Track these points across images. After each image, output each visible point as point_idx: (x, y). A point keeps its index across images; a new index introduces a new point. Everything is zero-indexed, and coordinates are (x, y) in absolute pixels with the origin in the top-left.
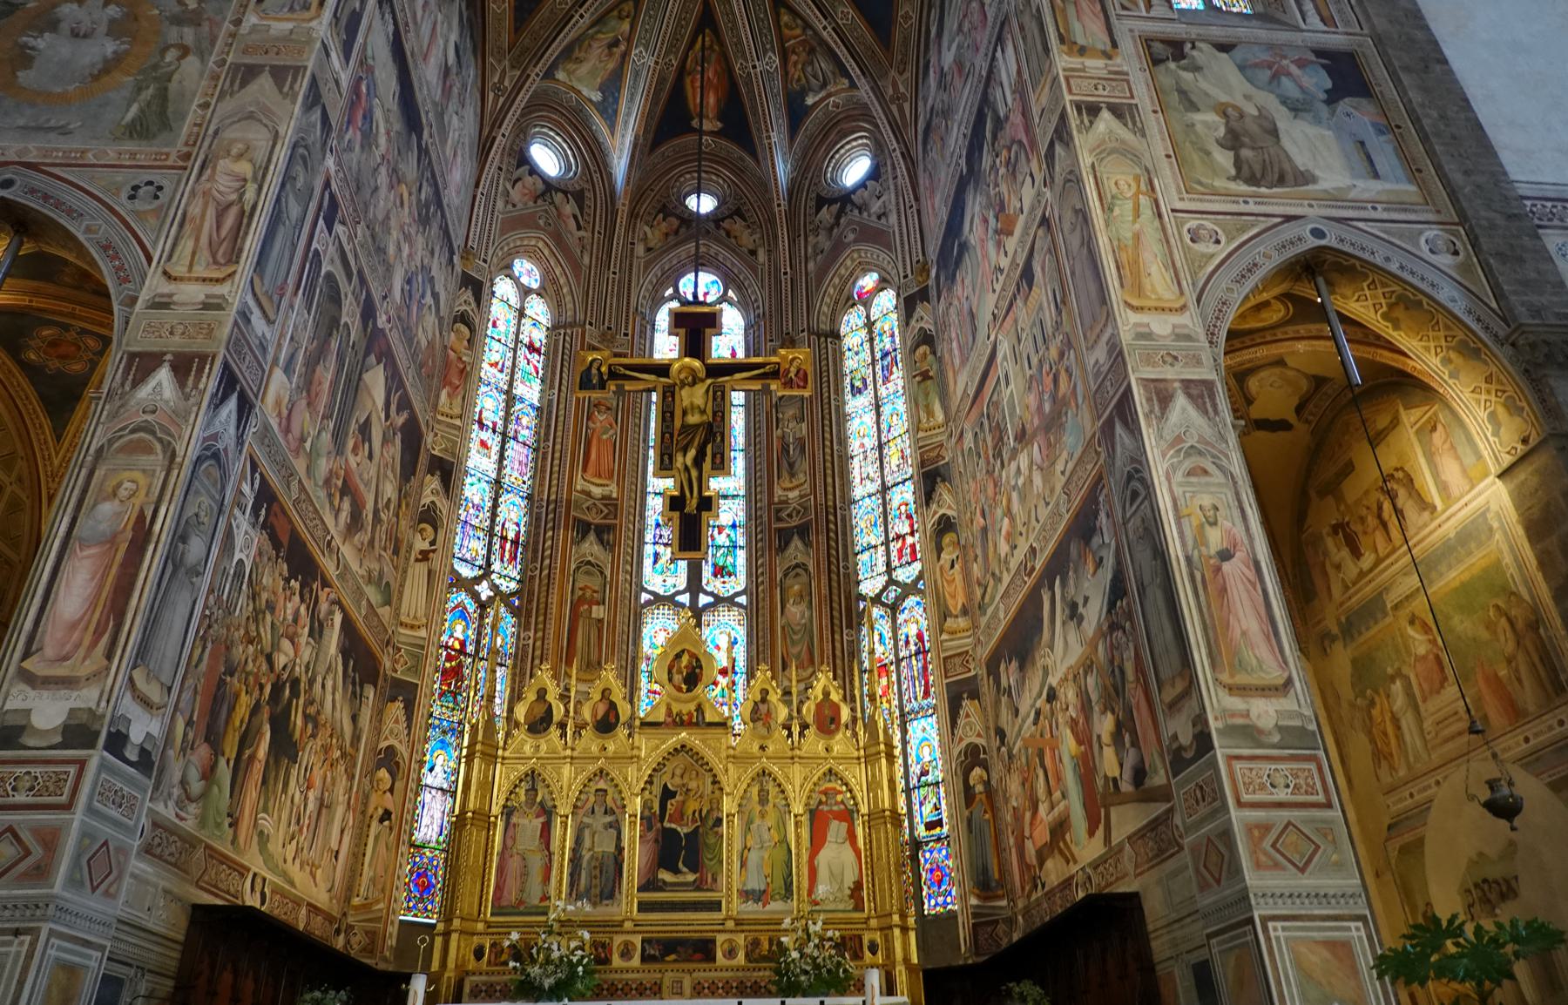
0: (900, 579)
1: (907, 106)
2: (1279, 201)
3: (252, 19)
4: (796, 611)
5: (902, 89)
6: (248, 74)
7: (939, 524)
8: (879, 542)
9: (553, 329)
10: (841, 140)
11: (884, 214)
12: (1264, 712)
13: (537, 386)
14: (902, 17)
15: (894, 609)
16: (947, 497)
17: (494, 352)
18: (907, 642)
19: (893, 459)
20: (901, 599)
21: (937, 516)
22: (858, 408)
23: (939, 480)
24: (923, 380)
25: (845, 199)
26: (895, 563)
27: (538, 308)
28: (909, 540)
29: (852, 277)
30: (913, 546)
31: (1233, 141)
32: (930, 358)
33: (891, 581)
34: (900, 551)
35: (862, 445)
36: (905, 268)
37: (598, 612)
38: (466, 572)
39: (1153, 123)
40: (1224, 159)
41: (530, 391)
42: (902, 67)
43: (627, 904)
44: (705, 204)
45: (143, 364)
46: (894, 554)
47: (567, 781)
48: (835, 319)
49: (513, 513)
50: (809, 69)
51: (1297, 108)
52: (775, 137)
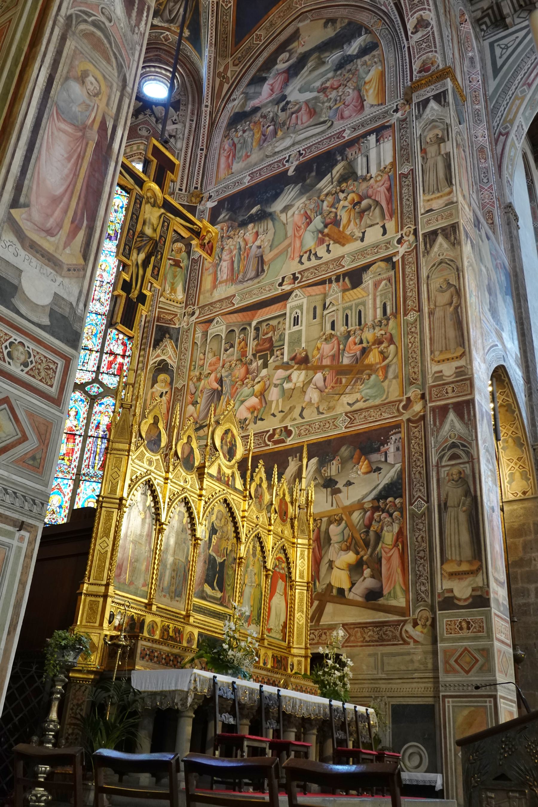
0: (105, 382)
1: (226, 87)
5: (229, 74)
7: (159, 364)
8: (95, 349)
10: (156, 61)
11: (174, 136)
14: (257, 35)
15: (93, 400)
16: (170, 350)
18: (98, 427)
20: (101, 396)
21: (159, 359)
23: (167, 336)
24: (174, 265)
26: (104, 369)
28: (120, 360)
30: (121, 365)
32: (184, 254)
33: (96, 380)
34: (110, 363)
35: (102, 276)
36: (181, 184)
42: (237, 62)
46: (104, 363)
50: (172, 4)
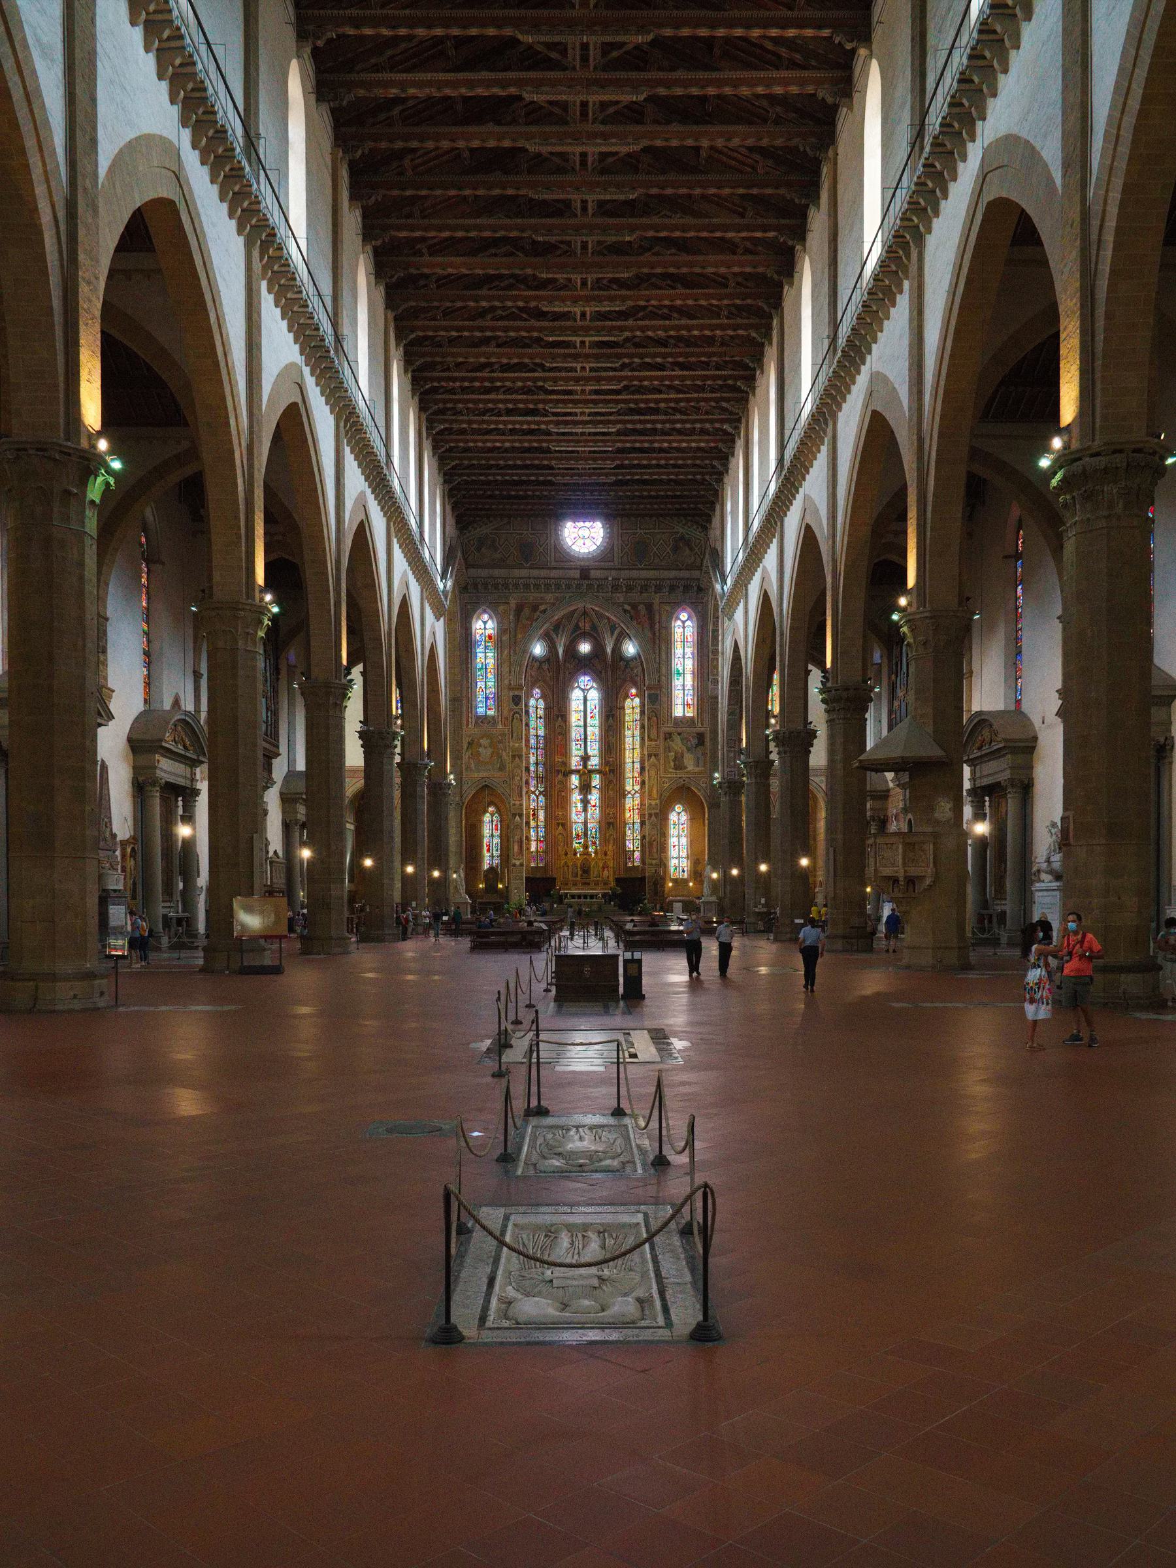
2: (679, 774)
3: (512, 744)
4: (611, 792)
6: (514, 756)
9: (545, 709)
12: (654, 862)
13: (543, 729)
17: (532, 724)
19: (636, 755)
22: (628, 733)
25: (627, 662)
27: (541, 704)
29: (628, 690)
31: (674, 760)
37: (563, 794)
38: (533, 789)
39: (662, 756)
40: (672, 764)
41: (541, 732)
43: (579, 879)
44: (585, 648)
45: (514, 815)
47: (570, 864)
48: (624, 702)
49: (540, 769)
51: (688, 750)
52: (607, 642)
